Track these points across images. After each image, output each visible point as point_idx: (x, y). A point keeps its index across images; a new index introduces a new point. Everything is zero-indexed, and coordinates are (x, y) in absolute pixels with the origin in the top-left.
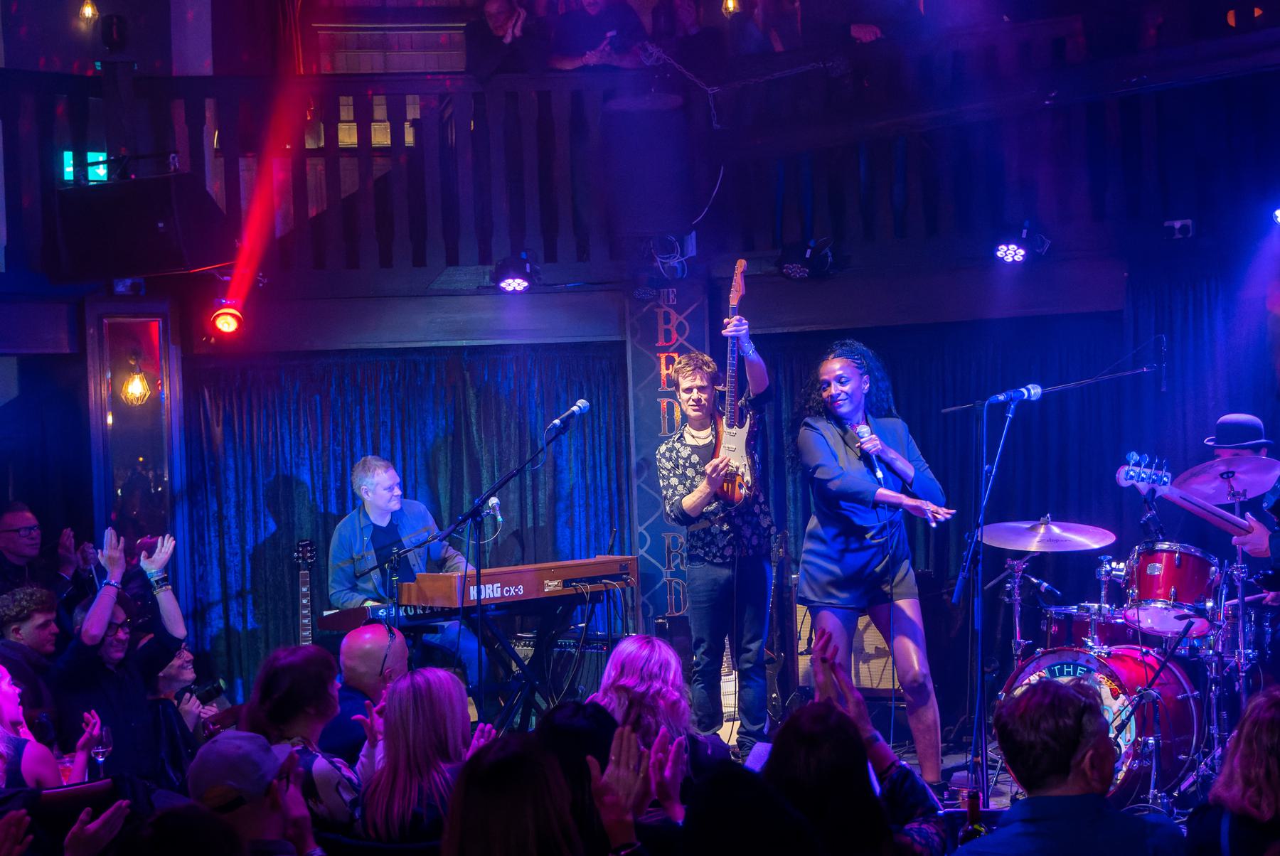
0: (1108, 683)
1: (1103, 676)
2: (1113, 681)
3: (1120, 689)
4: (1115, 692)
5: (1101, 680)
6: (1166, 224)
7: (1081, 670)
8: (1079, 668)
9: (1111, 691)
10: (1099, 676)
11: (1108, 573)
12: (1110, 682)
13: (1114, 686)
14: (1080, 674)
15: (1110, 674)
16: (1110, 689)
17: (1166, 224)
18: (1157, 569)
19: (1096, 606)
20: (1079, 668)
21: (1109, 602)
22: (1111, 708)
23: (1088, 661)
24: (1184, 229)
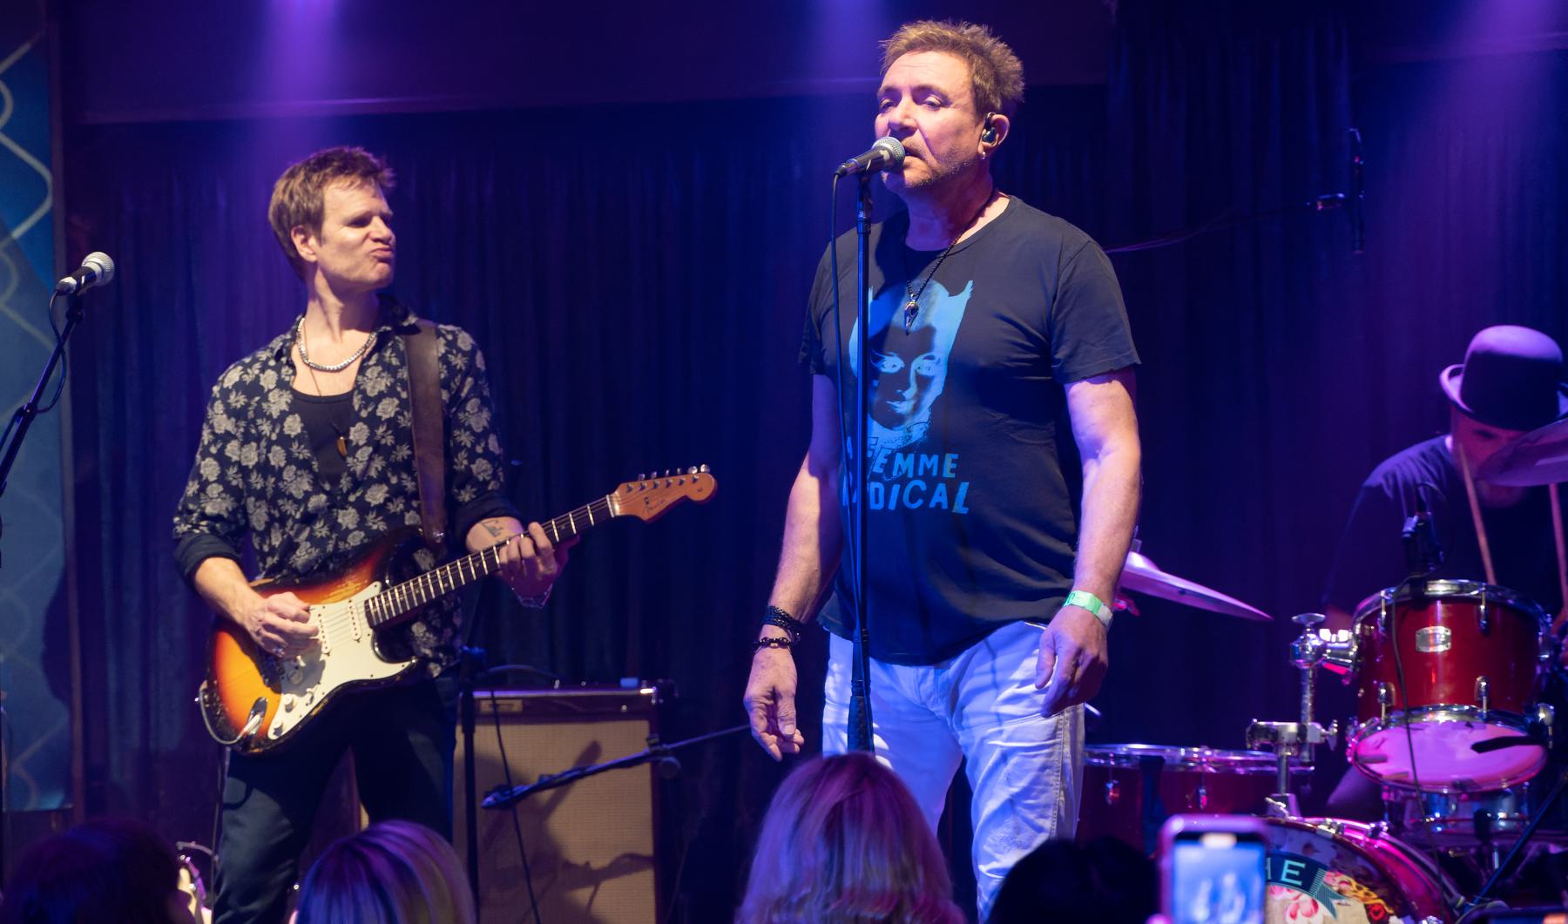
0: (1361, 894)
1: (1345, 878)
2: (1372, 889)
3: (1388, 904)
4: (1376, 913)
5: (1344, 886)
7: (1291, 867)
8: (1287, 863)
10: (1338, 879)
11: (1320, 650)
12: (1365, 889)
13: (1374, 899)
14: (1289, 876)
15: (1362, 872)
16: (1367, 907)
18: (1438, 639)
19: (1292, 727)
20: (1287, 863)
21: (1323, 718)
23: (1308, 847)
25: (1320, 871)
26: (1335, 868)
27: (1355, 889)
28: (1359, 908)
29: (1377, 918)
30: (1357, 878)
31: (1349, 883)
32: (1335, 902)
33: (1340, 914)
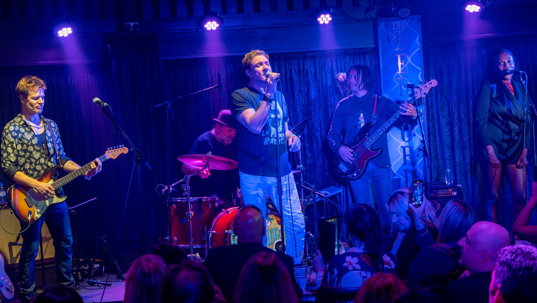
0: (276, 218)
1: (273, 216)
4: (279, 222)
5: (273, 217)
6: (126, 24)
9: (277, 222)
10: (271, 216)
12: (277, 217)
15: (276, 214)
16: (277, 221)
17: (126, 24)
22: (278, 228)
24: (135, 26)
25: (268, 215)
26: (271, 214)
27: (274, 217)
28: (276, 221)
29: (279, 223)
30: (275, 215)
31: (274, 217)
32: (271, 221)
33: (272, 223)
